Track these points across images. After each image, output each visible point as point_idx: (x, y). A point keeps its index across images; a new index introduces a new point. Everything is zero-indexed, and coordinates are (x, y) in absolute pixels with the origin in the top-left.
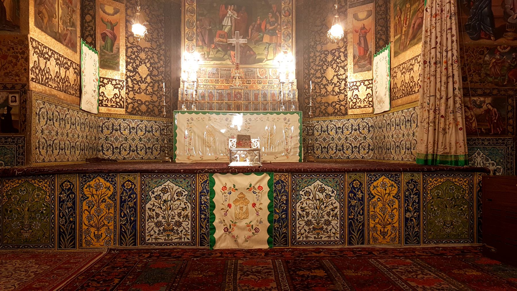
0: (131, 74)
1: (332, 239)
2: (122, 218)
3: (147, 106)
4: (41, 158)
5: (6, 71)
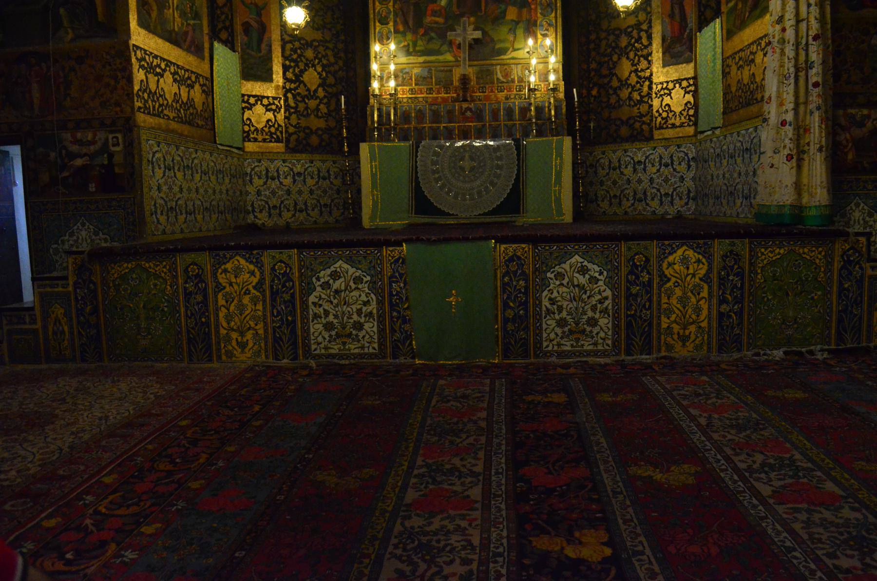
0: (293, 86)
1: (600, 347)
4: (160, 226)
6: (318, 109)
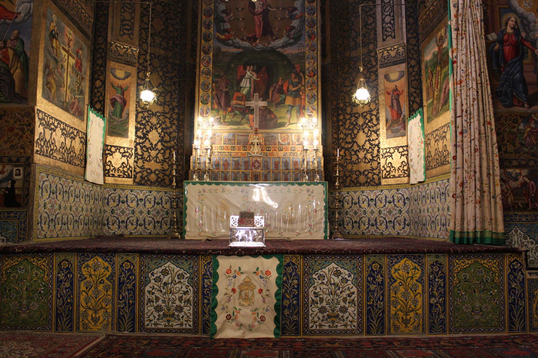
0: (141, 141)
1: (349, 327)
2: (121, 300)
3: (157, 175)
4: (43, 233)
5: (12, 144)
6: (157, 157)
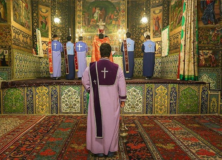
1: (139, 111)
4: (17, 77)
